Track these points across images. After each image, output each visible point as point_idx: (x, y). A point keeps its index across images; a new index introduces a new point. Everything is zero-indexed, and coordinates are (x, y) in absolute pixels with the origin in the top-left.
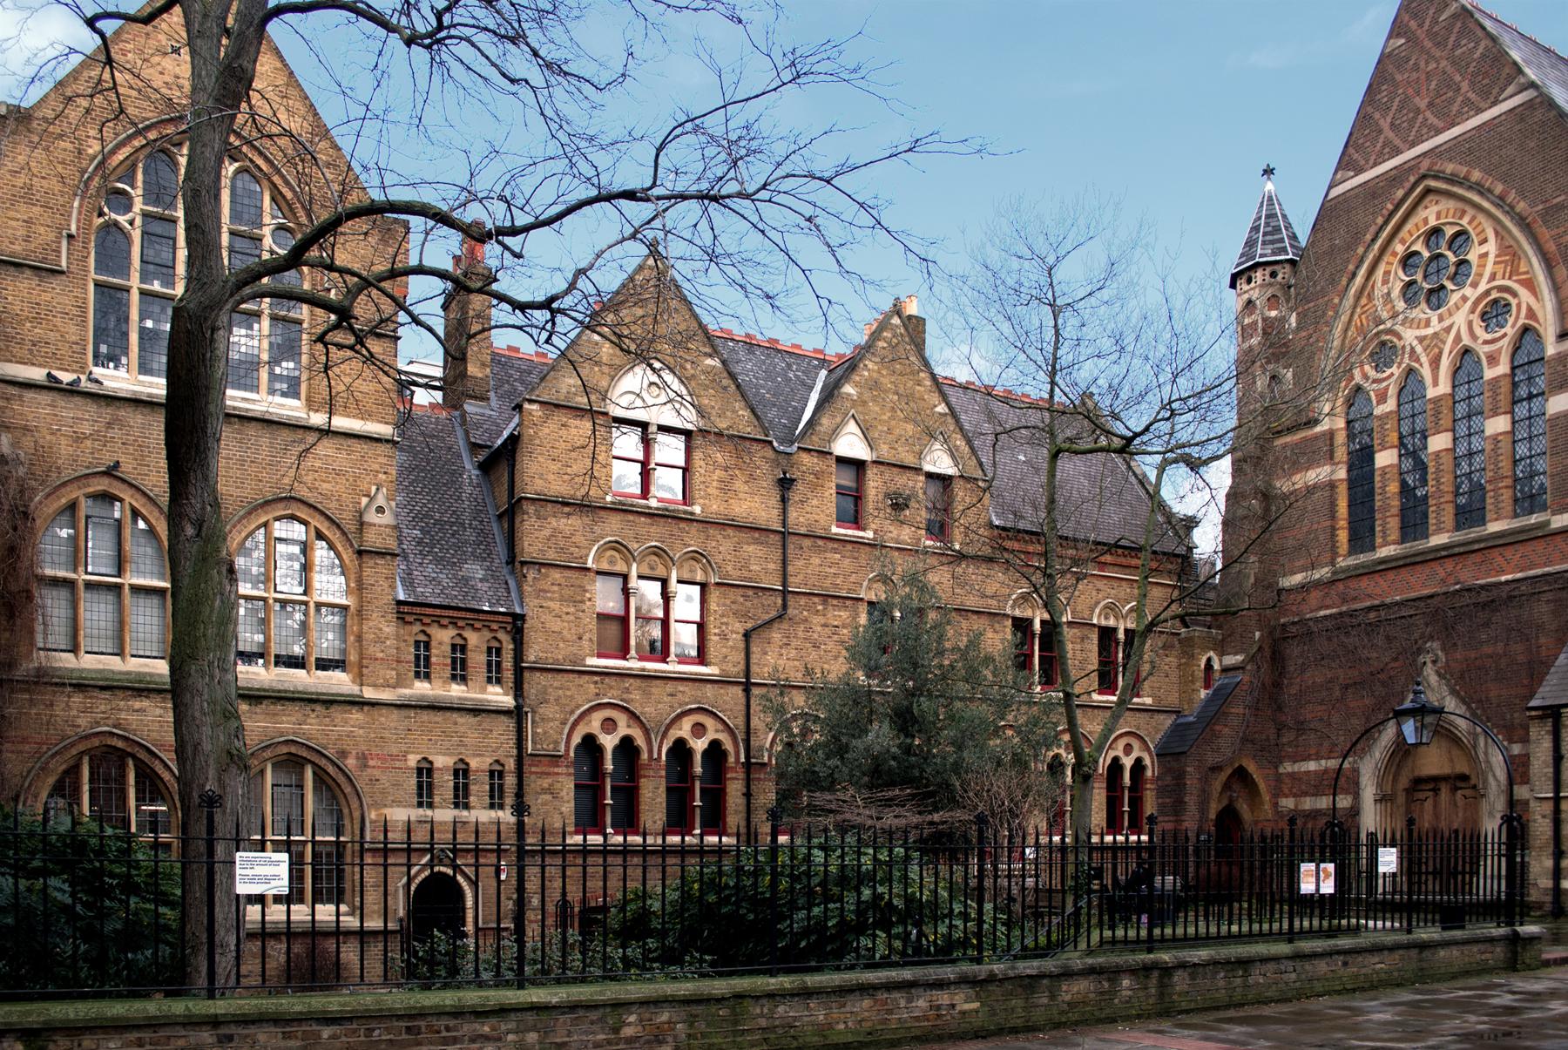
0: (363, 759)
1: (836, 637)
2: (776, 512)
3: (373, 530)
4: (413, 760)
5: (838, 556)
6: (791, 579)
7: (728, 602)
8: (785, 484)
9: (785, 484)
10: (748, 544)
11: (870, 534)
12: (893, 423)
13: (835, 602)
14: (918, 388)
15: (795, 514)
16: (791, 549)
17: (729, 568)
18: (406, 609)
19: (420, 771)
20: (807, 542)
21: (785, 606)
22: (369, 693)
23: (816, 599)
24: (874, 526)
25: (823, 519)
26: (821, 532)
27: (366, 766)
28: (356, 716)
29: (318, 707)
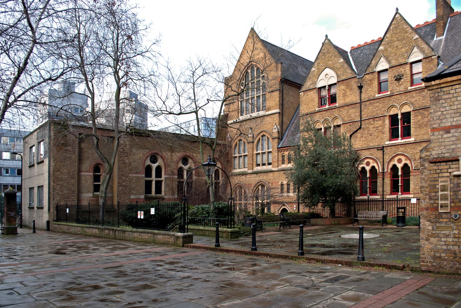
0: (272, 183)
1: (377, 131)
2: (358, 97)
3: (274, 134)
4: (280, 182)
5: (378, 104)
6: (362, 116)
7: (345, 128)
8: (360, 87)
9: (360, 87)
10: (351, 110)
11: (389, 93)
12: (397, 51)
13: (377, 119)
14: (406, 35)
15: (364, 96)
16: (363, 106)
17: (346, 118)
18: (279, 149)
19: (281, 185)
20: (368, 103)
21: (361, 125)
22: (273, 169)
23: (371, 120)
24: (390, 90)
25: (372, 94)
26: (372, 98)
27: (272, 185)
28: (271, 174)
29: (266, 173)
